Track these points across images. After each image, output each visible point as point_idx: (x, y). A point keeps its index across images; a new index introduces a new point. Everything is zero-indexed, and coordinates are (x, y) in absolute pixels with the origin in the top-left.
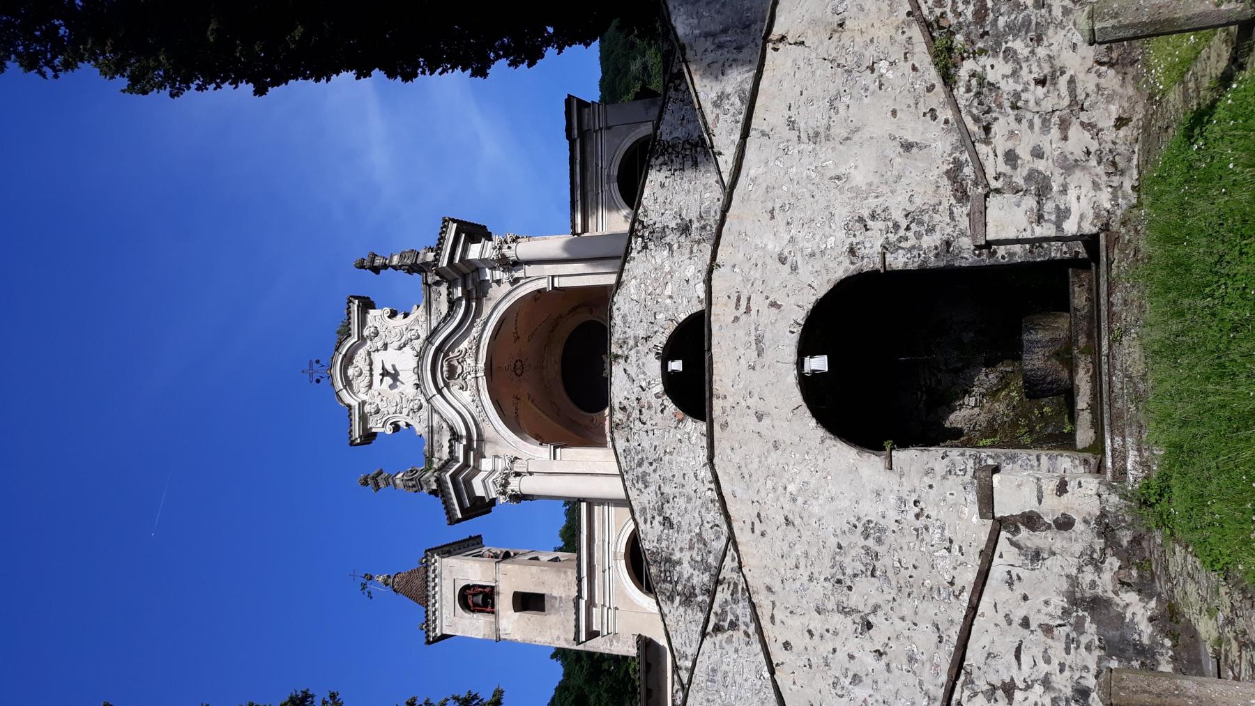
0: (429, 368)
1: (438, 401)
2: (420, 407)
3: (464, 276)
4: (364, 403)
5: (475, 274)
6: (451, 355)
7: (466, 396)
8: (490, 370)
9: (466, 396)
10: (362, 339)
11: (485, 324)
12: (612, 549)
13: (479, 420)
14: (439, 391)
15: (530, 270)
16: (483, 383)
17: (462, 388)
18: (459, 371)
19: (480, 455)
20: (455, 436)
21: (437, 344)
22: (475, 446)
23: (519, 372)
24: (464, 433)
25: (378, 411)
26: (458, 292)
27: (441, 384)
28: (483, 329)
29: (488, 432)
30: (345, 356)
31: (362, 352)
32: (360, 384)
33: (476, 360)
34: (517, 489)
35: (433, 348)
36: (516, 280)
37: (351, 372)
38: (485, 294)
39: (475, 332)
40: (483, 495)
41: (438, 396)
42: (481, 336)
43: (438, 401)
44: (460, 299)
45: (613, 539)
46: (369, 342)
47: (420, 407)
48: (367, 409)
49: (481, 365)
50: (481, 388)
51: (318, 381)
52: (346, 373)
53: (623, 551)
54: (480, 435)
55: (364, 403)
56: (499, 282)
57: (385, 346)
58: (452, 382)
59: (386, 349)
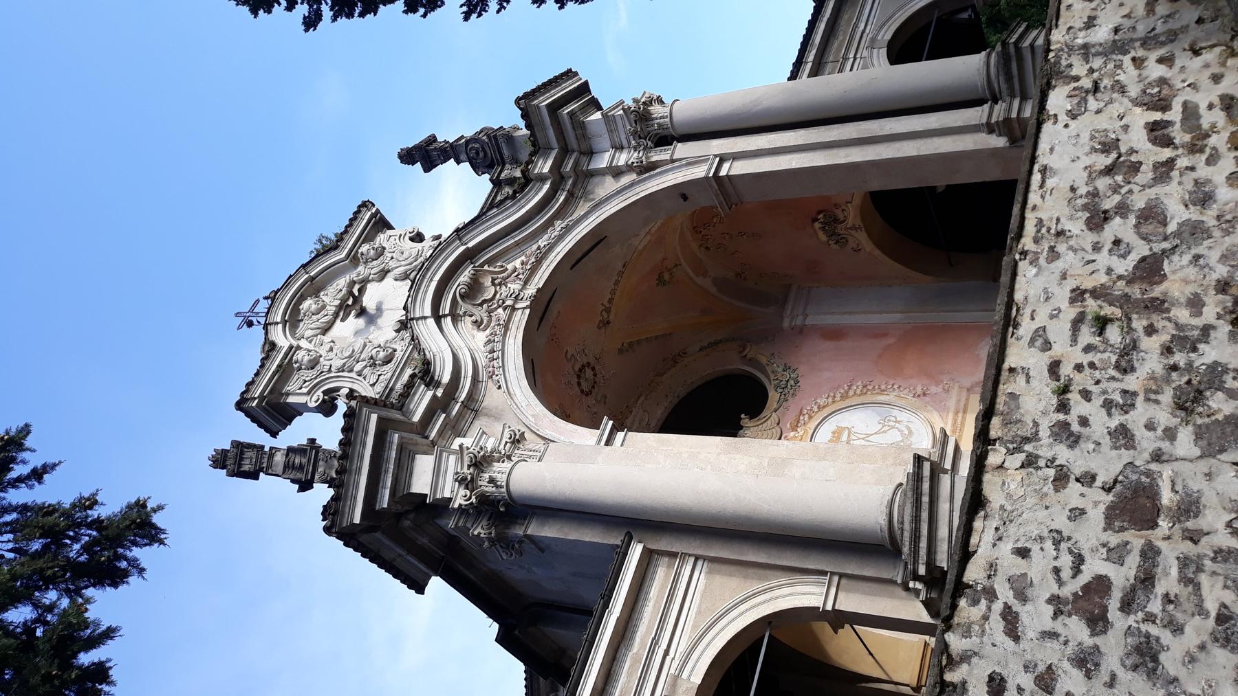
0: (437, 277)
1: (427, 331)
2: (388, 360)
3: (565, 151)
4: (299, 348)
5: (584, 159)
6: (486, 267)
7: (481, 337)
8: (542, 307)
9: (481, 337)
10: (354, 259)
11: (568, 230)
12: (671, 667)
13: (483, 375)
14: (438, 318)
15: (683, 150)
16: (520, 319)
17: (478, 324)
18: (488, 295)
19: (455, 428)
20: (426, 373)
21: (470, 245)
22: (457, 403)
23: (585, 386)
24: (446, 379)
25: (313, 364)
26: (544, 166)
27: (446, 308)
28: (560, 238)
29: (492, 397)
30: (312, 279)
31: (342, 282)
32: (307, 328)
33: (526, 283)
34: (501, 478)
35: (462, 248)
36: (652, 166)
37: (308, 304)
38: (586, 195)
39: (542, 242)
40: (426, 491)
41: (431, 322)
42: (551, 247)
43: (427, 331)
44: (542, 179)
45: (681, 645)
46: (361, 268)
47: (388, 360)
48: (300, 355)
49: (531, 290)
50: (513, 328)
51: (250, 324)
52: (300, 302)
53: (697, 679)
54: (471, 396)
55: (299, 348)
56: (617, 172)
57: (384, 274)
58: (464, 307)
59: (381, 279)
